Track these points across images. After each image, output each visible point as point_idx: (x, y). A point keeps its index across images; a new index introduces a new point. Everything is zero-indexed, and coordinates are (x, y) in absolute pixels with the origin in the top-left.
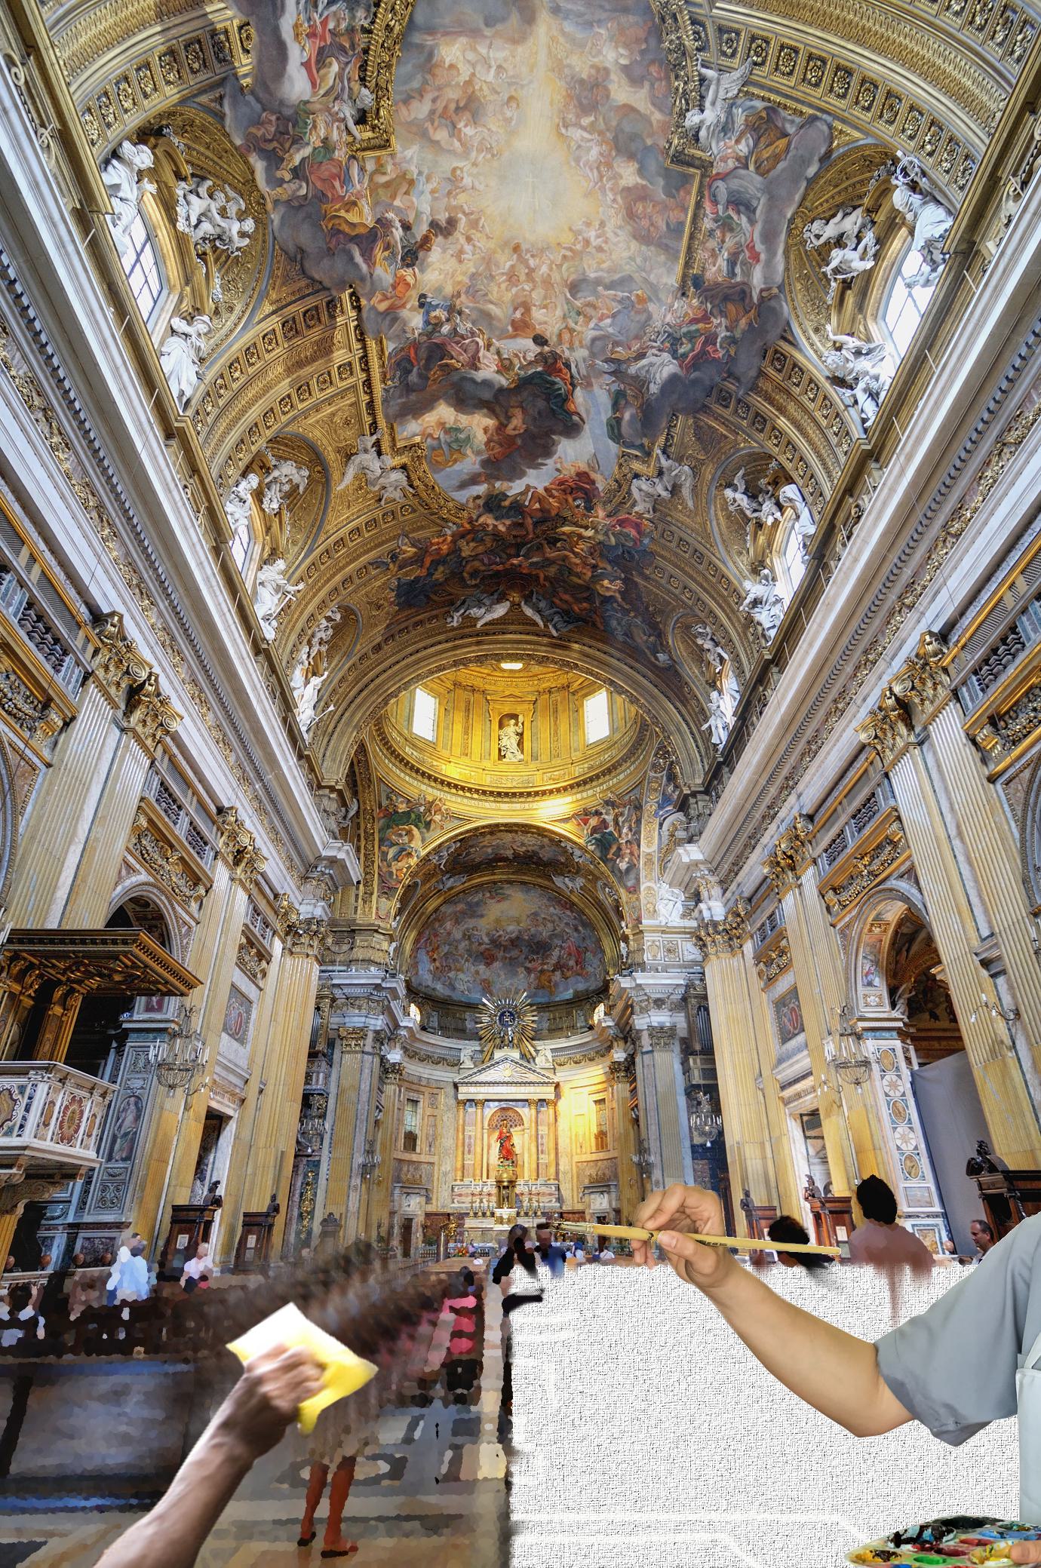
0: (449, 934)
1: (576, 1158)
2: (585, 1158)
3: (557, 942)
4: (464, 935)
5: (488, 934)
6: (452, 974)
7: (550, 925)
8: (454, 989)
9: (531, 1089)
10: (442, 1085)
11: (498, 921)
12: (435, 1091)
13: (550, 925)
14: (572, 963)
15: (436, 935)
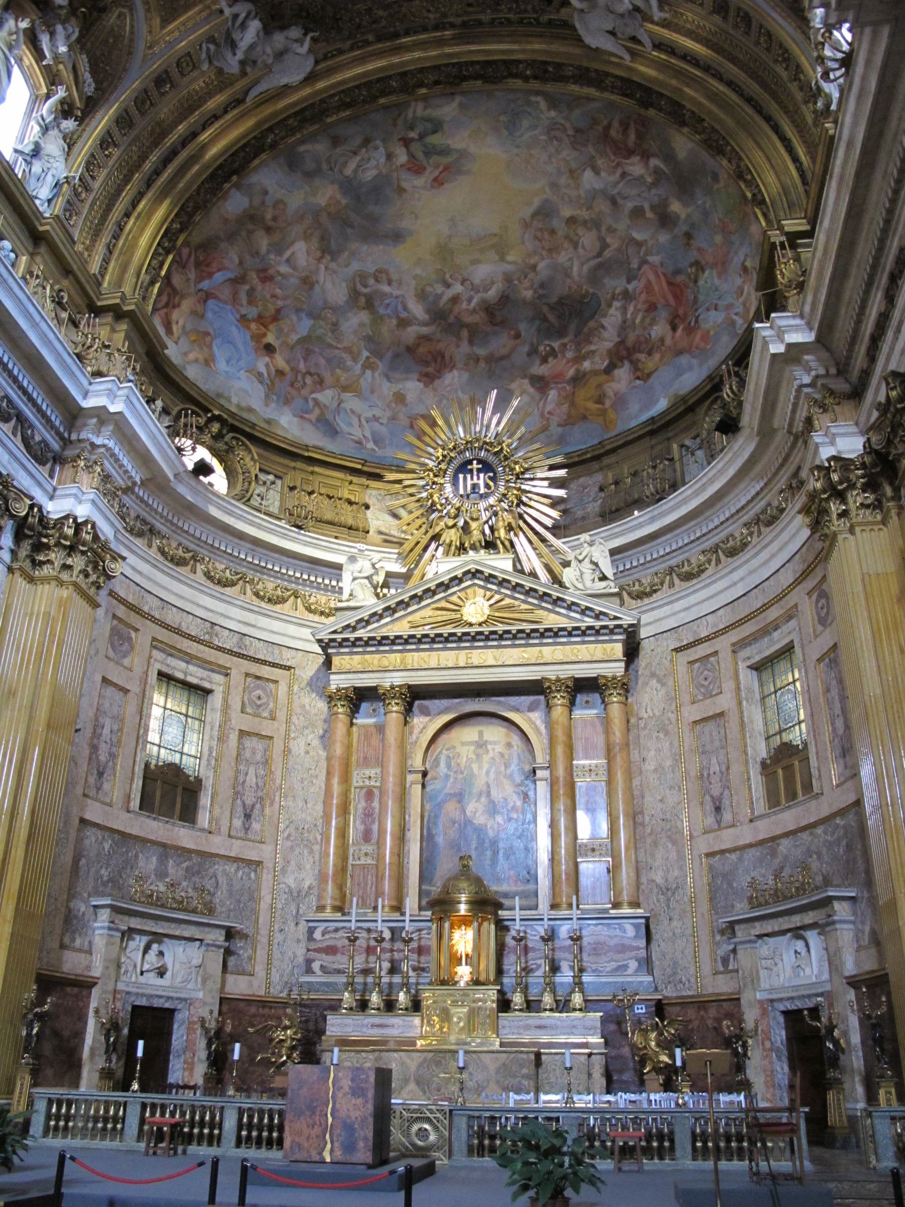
0: (308, 283)
1: (704, 845)
2: (727, 839)
3: (615, 283)
4: (354, 295)
5: (422, 295)
6: (326, 397)
7: (588, 239)
8: (333, 432)
9: (550, 652)
10: (287, 658)
11: (444, 251)
12: (266, 671)
13: (588, 239)
14: (659, 330)
15: (266, 277)
